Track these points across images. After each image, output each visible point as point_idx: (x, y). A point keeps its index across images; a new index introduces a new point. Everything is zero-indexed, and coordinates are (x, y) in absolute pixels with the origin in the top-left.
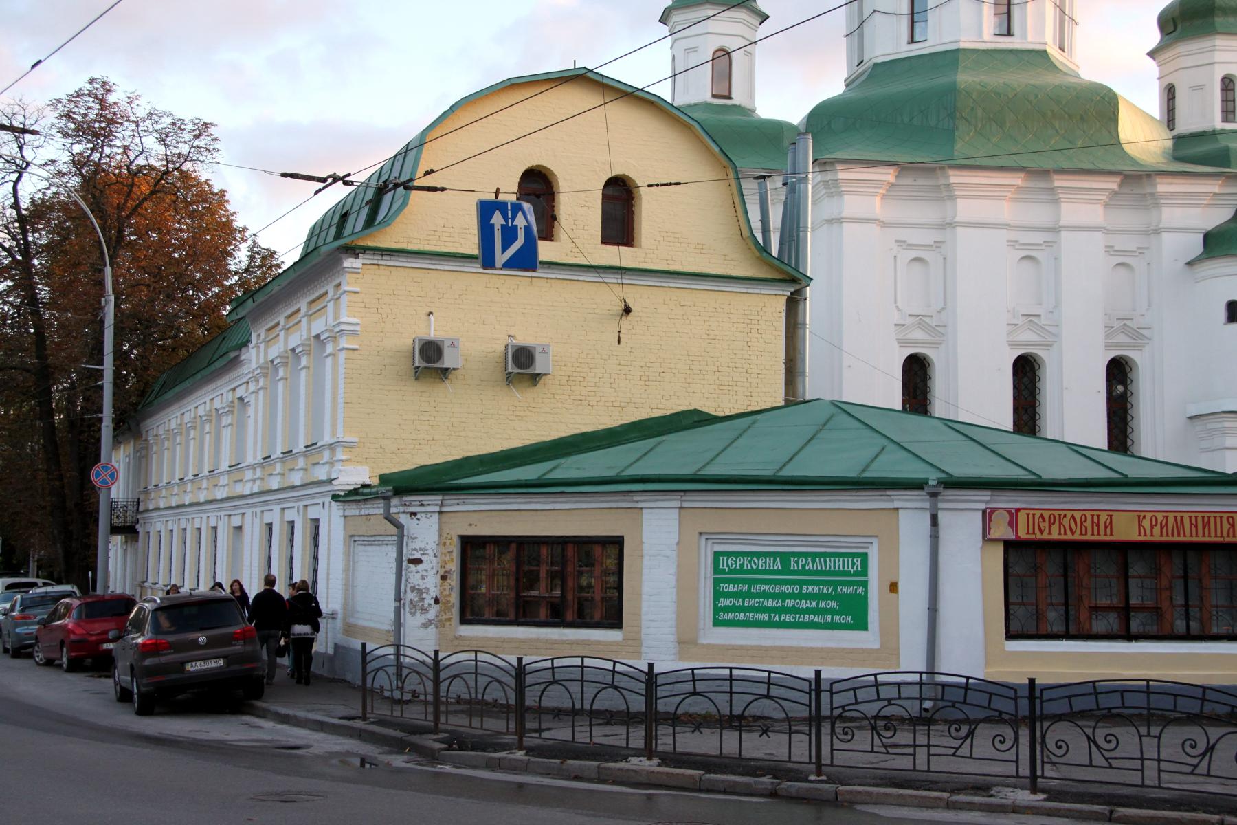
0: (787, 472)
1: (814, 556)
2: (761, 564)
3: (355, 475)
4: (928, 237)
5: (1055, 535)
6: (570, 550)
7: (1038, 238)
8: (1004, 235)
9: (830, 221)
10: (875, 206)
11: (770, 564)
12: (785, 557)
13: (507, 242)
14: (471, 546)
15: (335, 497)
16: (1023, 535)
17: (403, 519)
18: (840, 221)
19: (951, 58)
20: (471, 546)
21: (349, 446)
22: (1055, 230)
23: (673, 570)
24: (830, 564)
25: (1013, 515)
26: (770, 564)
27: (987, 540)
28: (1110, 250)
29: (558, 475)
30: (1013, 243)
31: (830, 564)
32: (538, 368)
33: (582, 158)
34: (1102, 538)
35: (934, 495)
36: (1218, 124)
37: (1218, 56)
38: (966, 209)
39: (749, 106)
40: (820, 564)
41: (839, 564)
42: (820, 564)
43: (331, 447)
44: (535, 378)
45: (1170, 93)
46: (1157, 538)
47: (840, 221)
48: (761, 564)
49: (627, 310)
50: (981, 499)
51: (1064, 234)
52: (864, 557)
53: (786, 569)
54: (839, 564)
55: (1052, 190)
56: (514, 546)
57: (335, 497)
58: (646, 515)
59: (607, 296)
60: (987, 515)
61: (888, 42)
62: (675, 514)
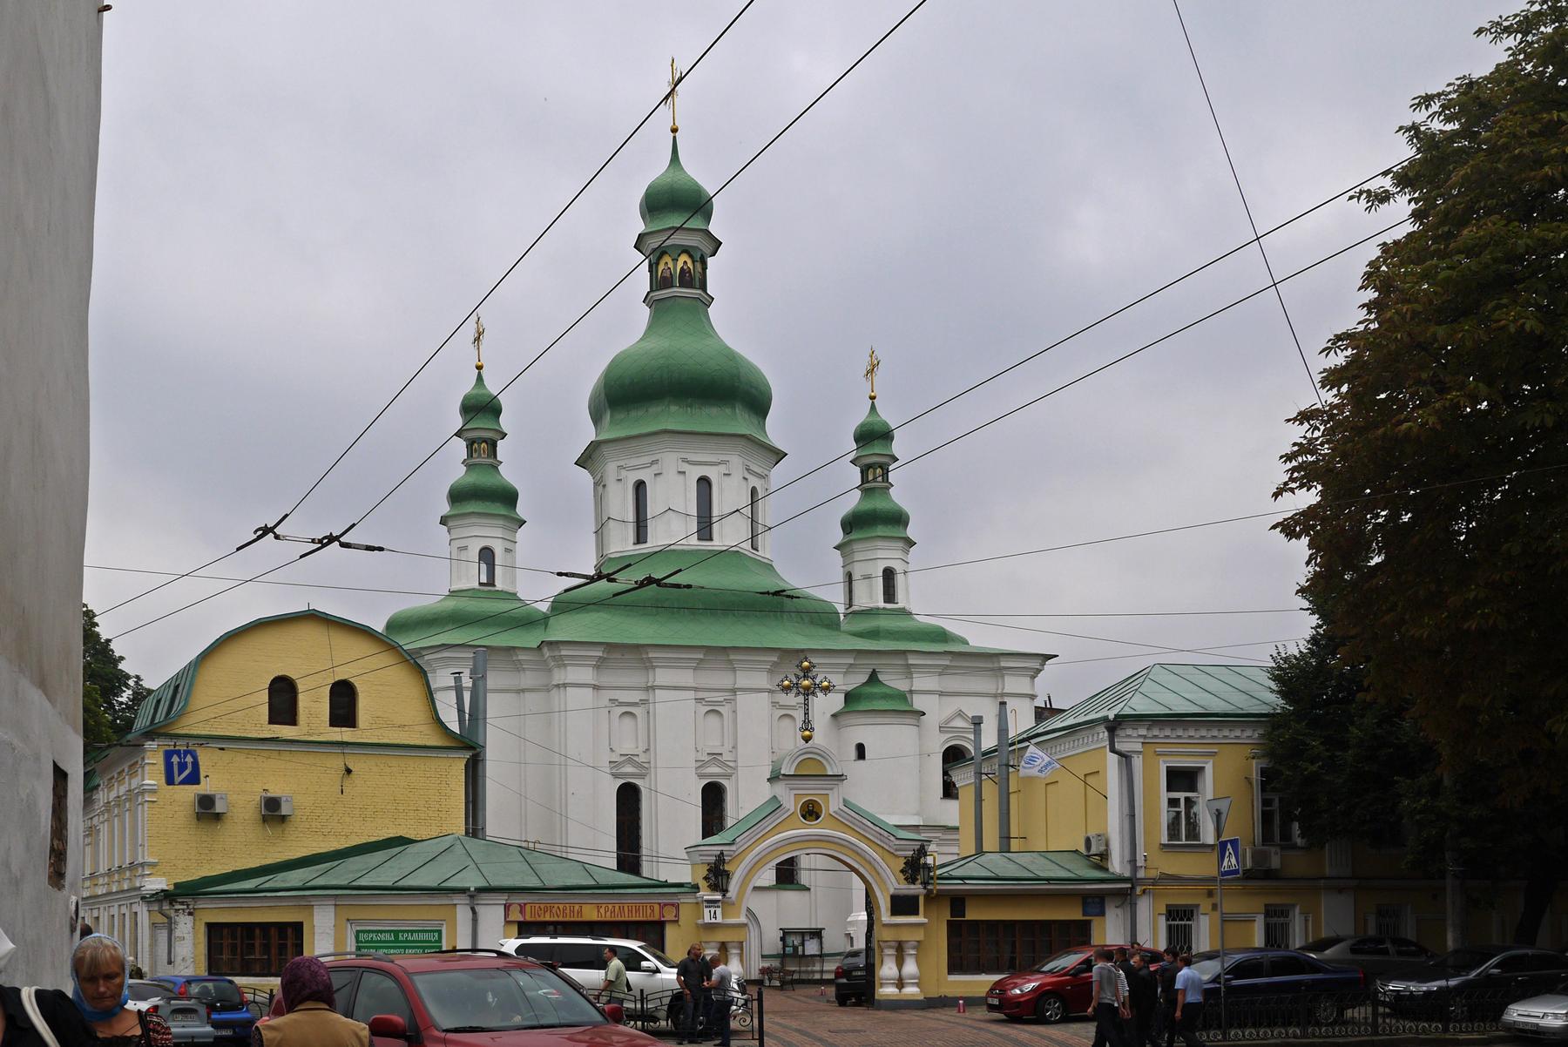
0: (400, 884)
1: (412, 932)
2: (382, 937)
3: (156, 883)
4: (635, 696)
5: (548, 918)
6: (273, 931)
7: (719, 697)
8: (691, 694)
9: (558, 686)
10: (586, 675)
11: (388, 937)
12: (396, 933)
13: (182, 766)
14: (212, 928)
15: (143, 898)
16: (528, 918)
17: (172, 913)
18: (565, 685)
19: (663, 553)
20: (212, 928)
21: (153, 865)
22: (734, 691)
23: (332, 941)
24: (422, 937)
25: (522, 908)
26: (388, 937)
27: (508, 922)
28: (774, 704)
29: (267, 885)
30: (699, 700)
31: (422, 937)
32: (284, 811)
33: (313, 666)
34: (576, 919)
35: (472, 897)
36: (881, 604)
37: (880, 554)
38: (662, 676)
39: (511, 590)
40: (415, 937)
41: (426, 937)
42: (415, 937)
43: (142, 865)
44: (283, 819)
45: (849, 578)
46: (608, 918)
47: (565, 685)
48: (382, 937)
49: (349, 771)
50: (502, 899)
51: (740, 697)
52: (440, 932)
53: (397, 940)
54: (426, 937)
55: (730, 662)
56: (257, 931)
57: (143, 898)
58: (316, 910)
59: (336, 762)
60: (507, 907)
61: (622, 543)
62: (332, 909)
